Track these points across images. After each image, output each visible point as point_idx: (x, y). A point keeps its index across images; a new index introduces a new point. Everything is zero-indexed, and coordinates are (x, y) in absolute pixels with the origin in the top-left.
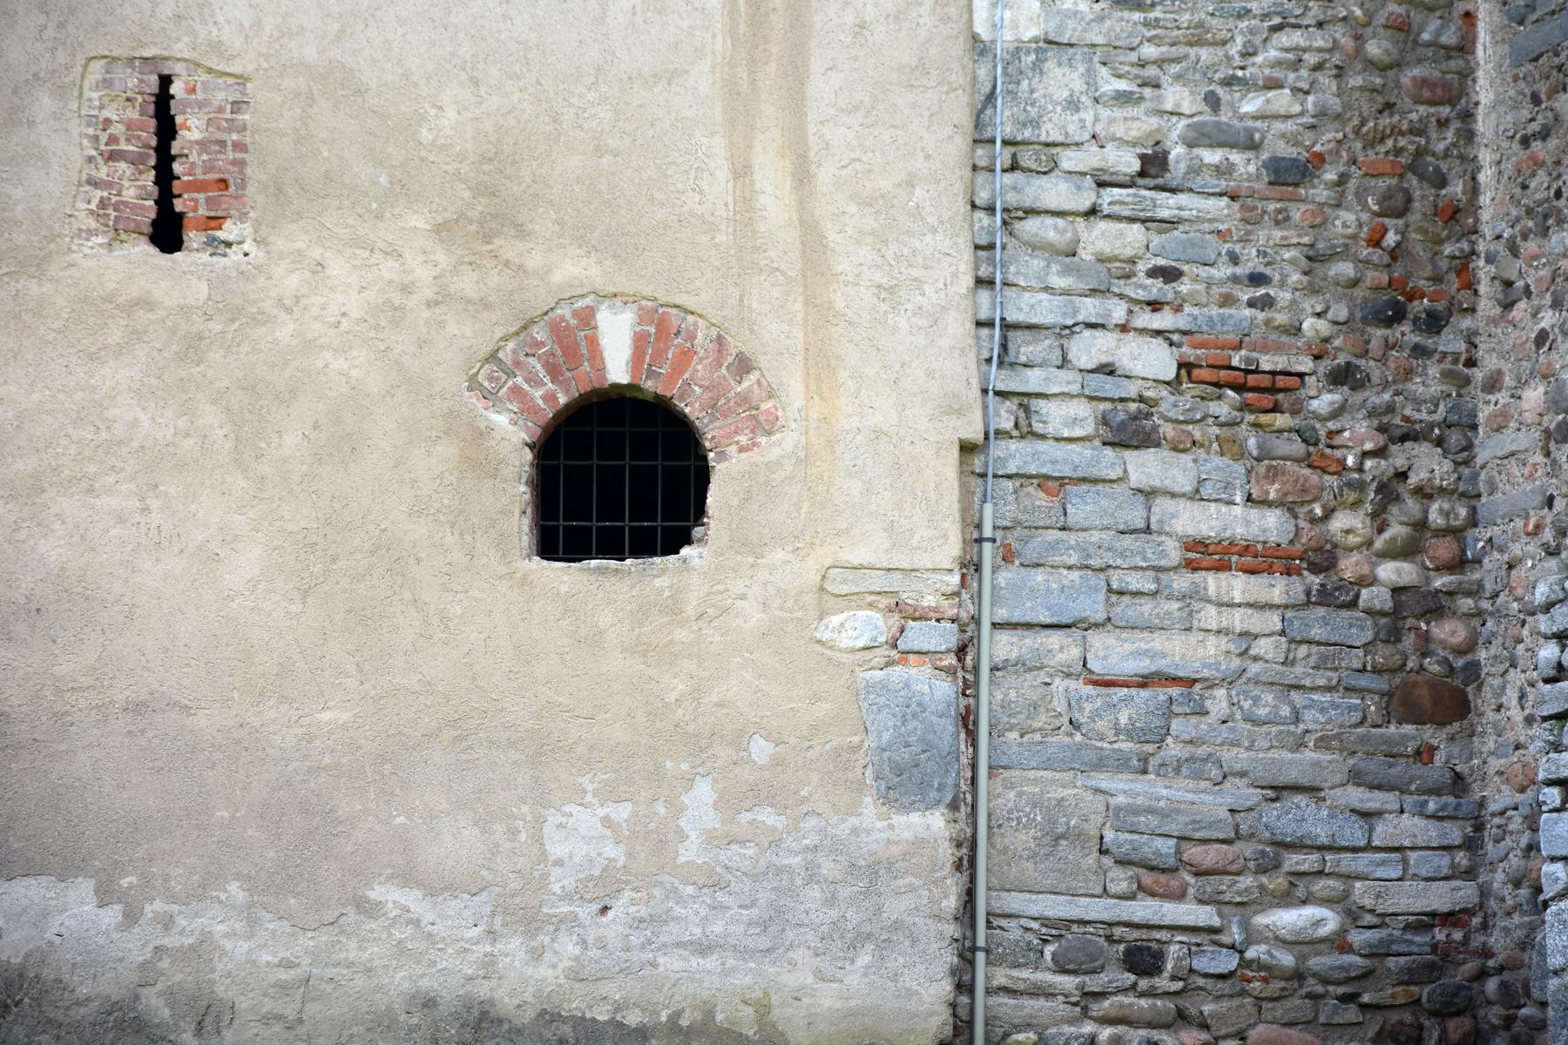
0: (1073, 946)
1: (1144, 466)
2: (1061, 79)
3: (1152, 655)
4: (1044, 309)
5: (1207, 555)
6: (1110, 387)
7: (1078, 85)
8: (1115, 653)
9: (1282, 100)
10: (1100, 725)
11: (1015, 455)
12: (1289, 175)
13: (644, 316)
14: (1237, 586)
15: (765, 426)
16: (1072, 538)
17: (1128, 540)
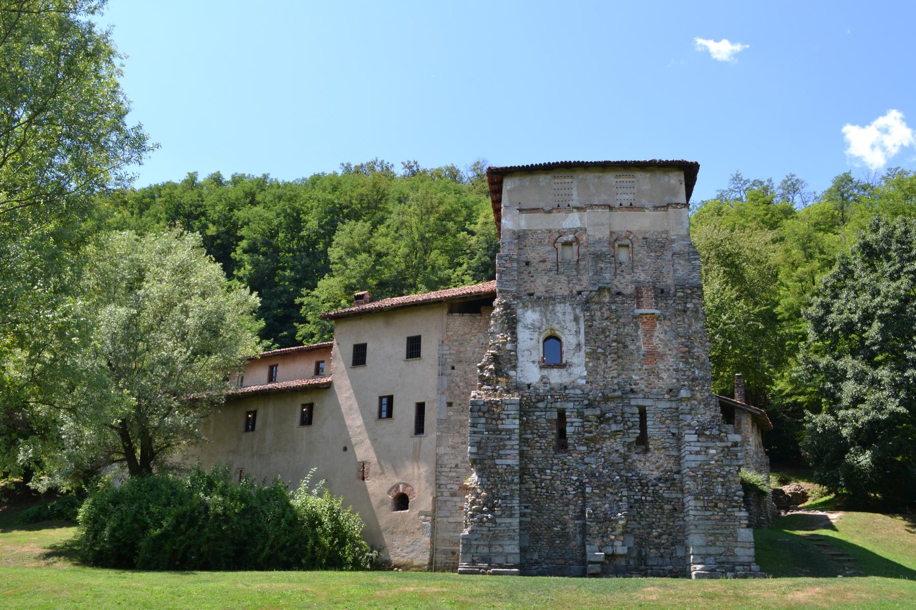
0: (445, 552)
1: (455, 499)
2: (446, 457)
8: (451, 520)
11: (440, 498)
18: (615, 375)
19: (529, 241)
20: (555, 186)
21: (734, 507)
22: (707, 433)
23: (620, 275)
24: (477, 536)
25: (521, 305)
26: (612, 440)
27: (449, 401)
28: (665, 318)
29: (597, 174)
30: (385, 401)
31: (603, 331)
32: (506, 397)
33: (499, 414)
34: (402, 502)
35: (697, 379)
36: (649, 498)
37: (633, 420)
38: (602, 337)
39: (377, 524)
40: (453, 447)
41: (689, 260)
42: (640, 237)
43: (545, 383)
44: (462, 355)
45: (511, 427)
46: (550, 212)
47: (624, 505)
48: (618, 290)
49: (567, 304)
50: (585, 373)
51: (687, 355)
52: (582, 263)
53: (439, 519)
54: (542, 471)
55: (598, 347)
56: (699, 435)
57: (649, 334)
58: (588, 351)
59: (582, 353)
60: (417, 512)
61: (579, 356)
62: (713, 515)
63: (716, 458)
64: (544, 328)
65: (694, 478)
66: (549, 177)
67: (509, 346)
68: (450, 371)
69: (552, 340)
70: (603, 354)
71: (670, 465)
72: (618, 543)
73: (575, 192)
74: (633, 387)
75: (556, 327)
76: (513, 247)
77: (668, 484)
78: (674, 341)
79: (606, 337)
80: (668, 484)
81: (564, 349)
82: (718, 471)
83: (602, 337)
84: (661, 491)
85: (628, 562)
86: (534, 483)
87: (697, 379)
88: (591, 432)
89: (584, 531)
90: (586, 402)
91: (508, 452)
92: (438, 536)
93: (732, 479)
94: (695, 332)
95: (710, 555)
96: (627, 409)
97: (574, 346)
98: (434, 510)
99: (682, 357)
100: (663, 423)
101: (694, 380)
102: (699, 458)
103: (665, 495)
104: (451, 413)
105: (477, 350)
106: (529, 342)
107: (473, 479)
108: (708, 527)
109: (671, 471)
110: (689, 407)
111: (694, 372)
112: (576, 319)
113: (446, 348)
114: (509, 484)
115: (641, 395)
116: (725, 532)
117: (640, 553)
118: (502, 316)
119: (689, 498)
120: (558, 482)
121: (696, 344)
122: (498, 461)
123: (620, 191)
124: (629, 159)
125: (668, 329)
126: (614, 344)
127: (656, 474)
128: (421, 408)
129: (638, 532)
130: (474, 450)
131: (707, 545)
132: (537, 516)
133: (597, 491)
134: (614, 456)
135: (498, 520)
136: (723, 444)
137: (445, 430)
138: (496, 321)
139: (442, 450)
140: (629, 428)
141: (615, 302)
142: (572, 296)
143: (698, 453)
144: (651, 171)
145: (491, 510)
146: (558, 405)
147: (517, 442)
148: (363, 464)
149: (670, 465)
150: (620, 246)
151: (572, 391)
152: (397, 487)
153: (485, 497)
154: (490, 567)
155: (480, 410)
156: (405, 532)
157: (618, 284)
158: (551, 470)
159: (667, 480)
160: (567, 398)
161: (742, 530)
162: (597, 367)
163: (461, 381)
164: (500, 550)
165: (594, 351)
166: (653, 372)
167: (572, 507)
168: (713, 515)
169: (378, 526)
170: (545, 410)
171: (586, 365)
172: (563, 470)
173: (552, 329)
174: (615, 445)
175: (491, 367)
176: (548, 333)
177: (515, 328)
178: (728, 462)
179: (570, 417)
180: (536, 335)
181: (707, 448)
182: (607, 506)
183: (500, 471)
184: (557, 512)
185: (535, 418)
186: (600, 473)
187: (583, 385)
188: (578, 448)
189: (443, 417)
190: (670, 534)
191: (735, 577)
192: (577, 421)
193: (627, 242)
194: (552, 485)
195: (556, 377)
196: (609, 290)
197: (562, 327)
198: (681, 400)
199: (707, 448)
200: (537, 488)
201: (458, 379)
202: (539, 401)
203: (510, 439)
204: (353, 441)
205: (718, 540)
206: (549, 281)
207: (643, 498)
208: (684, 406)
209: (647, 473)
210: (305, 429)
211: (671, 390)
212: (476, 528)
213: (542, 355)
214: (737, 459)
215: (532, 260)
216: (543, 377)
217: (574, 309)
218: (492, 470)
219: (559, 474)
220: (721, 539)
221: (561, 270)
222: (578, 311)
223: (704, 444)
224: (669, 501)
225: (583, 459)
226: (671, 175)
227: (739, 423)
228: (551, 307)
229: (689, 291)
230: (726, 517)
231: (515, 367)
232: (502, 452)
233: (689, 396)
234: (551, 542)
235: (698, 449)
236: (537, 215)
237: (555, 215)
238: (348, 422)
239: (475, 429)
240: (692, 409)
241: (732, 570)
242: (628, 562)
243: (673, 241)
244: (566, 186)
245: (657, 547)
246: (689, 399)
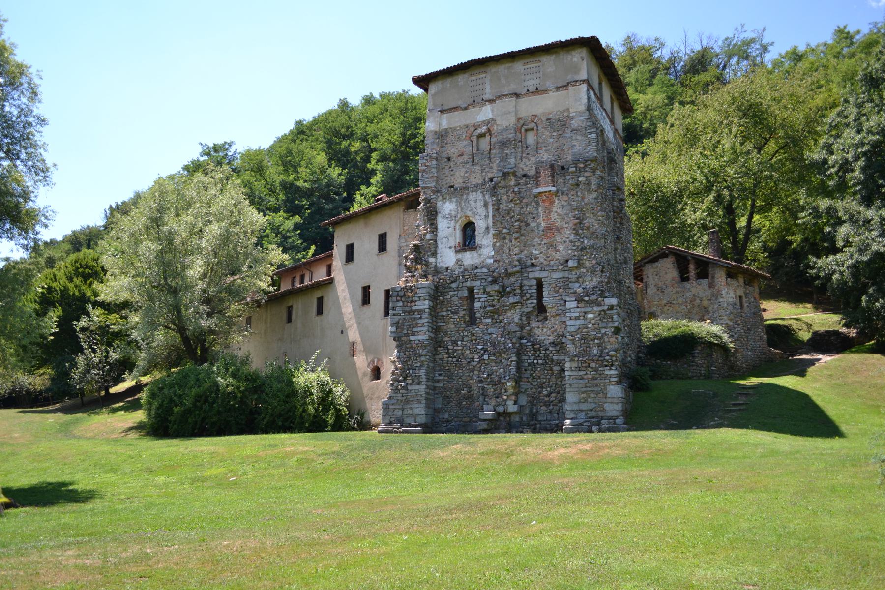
19: (450, 138)
20: (472, 84)
21: (606, 366)
23: (526, 158)
24: (393, 401)
25: (441, 198)
28: (563, 194)
29: (507, 65)
34: (376, 373)
35: (585, 248)
36: (540, 362)
37: (530, 291)
41: (585, 135)
42: (544, 119)
46: (466, 108)
48: (523, 173)
50: (493, 253)
51: (579, 226)
52: (493, 152)
54: (455, 343)
55: (504, 228)
57: (548, 211)
59: (491, 235)
62: (586, 374)
63: (593, 321)
64: (459, 216)
66: (466, 75)
72: (510, 403)
73: (488, 86)
74: (534, 261)
75: (469, 213)
76: (435, 146)
77: (558, 348)
80: (558, 348)
85: (521, 418)
86: (447, 353)
91: (419, 329)
94: (586, 204)
95: (582, 411)
100: (557, 292)
102: (578, 322)
103: (554, 358)
106: (448, 232)
111: (583, 242)
112: (486, 205)
113: (403, 241)
116: (596, 389)
117: (531, 409)
120: (468, 352)
121: (587, 215)
122: (412, 338)
123: (528, 77)
124: (532, 46)
127: (551, 339)
129: (530, 391)
130: (394, 329)
131: (580, 402)
134: (513, 327)
135: (409, 388)
136: (600, 308)
140: (528, 299)
141: (519, 184)
142: (484, 184)
143: (577, 318)
144: (556, 52)
146: (468, 284)
148: (353, 343)
150: (526, 130)
152: (373, 362)
154: (402, 426)
157: (523, 167)
158: (462, 341)
160: (475, 277)
161: (612, 387)
164: (410, 412)
167: (476, 372)
168: (586, 374)
170: (457, 289)
171: (494, 245)
172: (472, 341)
173: (466, 217)
174: (514, 316)
175: (412, 256)
177: (435, 219)
178: (604, 325)
179: (478, 293)
180: (453, 223)
181: (585, 313)
182: (502, 370)
191: (600, 431)
192: (483, 296)
193: (533, 125)
195: (469, 259)
196: (514, 174)
197: (474, 213)
199: (585, 313)
202: (452, 282)
203: (421, 318)
204: (347, 325)
206: (466, 172)
210: (319, 317)
214: (613, 321)
215: (452, 156)
216: (458, 260)
217: (484, 196)
220: (592, 396)
221: (476, 161)
222: (487, 197)
223: (583, 310)
226: (573, 53)
227: (713, 277)
228: (465, 196)
229: (582, 165)
231: (434, 254)
232: (414, 330)
234: (459, 404)
235: (577, 314)
236: (456, 113)
237: (472, 110)
238: (344, 310)
241: (599, 424)
242: (521, 418)
243: (572, 118)
244: (481, 81)
245: (547, 404)
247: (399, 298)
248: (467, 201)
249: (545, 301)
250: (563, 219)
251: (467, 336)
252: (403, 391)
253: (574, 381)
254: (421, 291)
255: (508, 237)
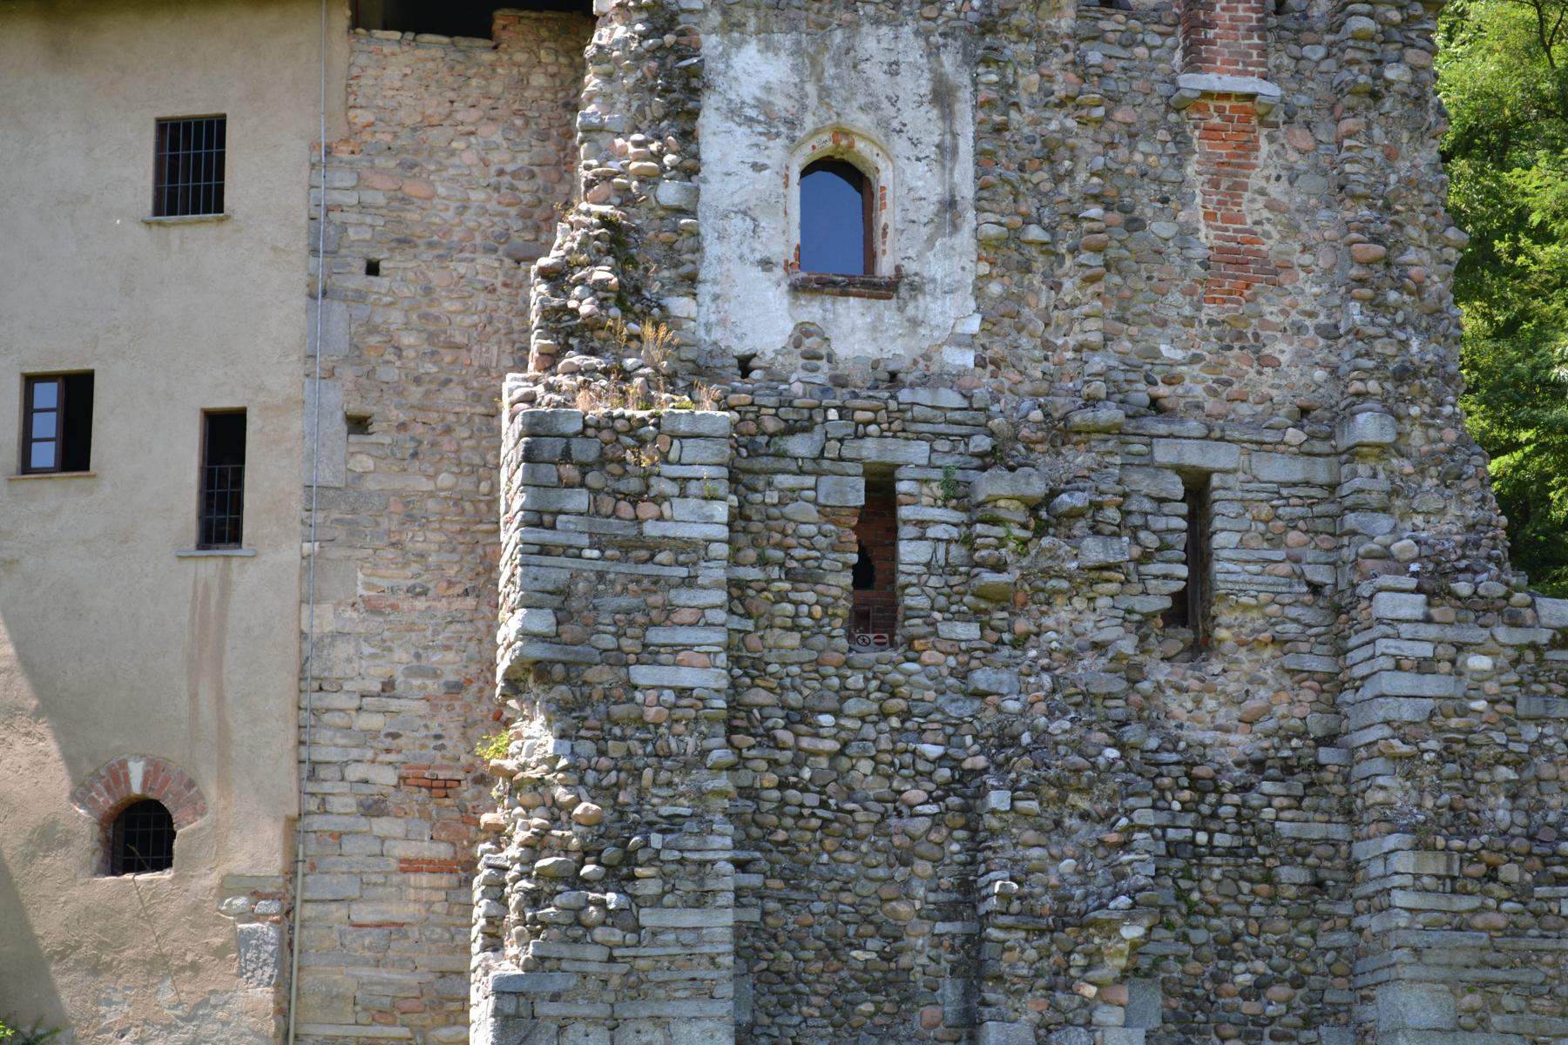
1: (381, 825)
2: (343, 649)
3: (383, 913)
4: (332, 754)
5: (410, 866)
6: (365, 789)
7: (352, 651)
8: (364, 913)
9: (450, 656)
10: (355, 946)
11: (317, 822)
12: (455, 689)
13: (150, 763)
14: (424, 879)
15: (202, 812)
16: (343, 860)
17: (371, 860)
18: (1096, 338)
22: (1463, 588)
24: (558, 982)
26: (1079, 603)
27: (357, 408)
28: (1290, 120)
30: (47, 395)
31: (1049, 157)
32: (670, 404)
33: (646, 476)
35: (1415, 373)
37: (1160, 523)
38: (1041, 176)
39: (26, 926)
40: (373, 609)
43: (812, 356)
44: (412, 216)
45: (697, 531)
47: (1140, 864)
49: (907, 31)
50: (974, 325)
51: (1377, 278)
53: (309, 911)
54: (800, 717)
55: (1027, 221)
56: (1431, 595)
57: (1229, 179)
58: (992, 231)
59: (964, 240)
60: (213, 880)
61: (949, 253)
63: (1492, 688)
64: (810, 122)
65: (1407, 765)
67: (669, 192)
68: (360, 280)
69: (841, 174)
70: (1046, 248)
71: (1298, 708)
74: (1162, 390)
75: (861, 121)
77: (1297, 785)
78: (1323, 215)
79: (1058, 179)
80: (1297, 785)
81: (887, 216)
82: (1500, 738)
83: (1041, 176)
84: (1268, 813)
86: (773, 764)
87: (1415, 373)
88: (999, 567)
89: (973, 965)
90: (982, 443)
91: (682, 636)
92: (308, 980)
93: (1548, 771)
94: (1408, 183)
96: (1141, 481)
97: (929, 210)
98: (291, 874)
99: (1361, 282)
100: (1275, 541)
101: (1404, 374)
103: (1286, 829)
104: (364, 463)
105: (477, 196)
106: (745, 180)
107: (532, 740)
108: (1461, 958)
109: (1303, 735)
110: (1382, 483)
111: (1404, 344)
112: (942, 96)
114: (687, 768)
115: (1194, 426)
116: (1524, 975)
118: (638, 58)
119: (1392, 841)
120: (865, 766)
121: (1412, 231)
122: (642, 674)
125: (1302, 164)
126: (1095, 211)
127: (1242, 743)
128: (225, 435)
129: (1176, 970)
130: (544, 622)
132: (785, 902)
133: (1033, 805)
135: (648, 918)
137: (340, 533)
138: (609, 77)
139: (324, 619)
140: (1146, 557)
141: (1098, 37)
143: (1423, 666)
145: (620, 874)
146: (871, 449)
147: (720, 597)
149: (1298, 708)
151: (923, 396)
153: (590, 822)
155: (566, 456)
156: (158, 966)
158: (837, 713)
159: (1288, 770)
160: (901, 424)
162: (1020, 299)
163: (407, 326)
165: (1014, 237)
166: (1240, 336)
167: (923, 868)
168: (1483, 909)
169: (31, 940)
171: (978, 291)
172: (884, 715)
173: (839, 132)
175: (601, 273)
176: (823, 145)
177: (694, 115)
178: (1536, 706)
179: (914, 500)
180: (777, 148)
181: (1460, 647)
182: (1068, 865)
183: (651, 713)
184: (866, 888)
185: (772, 497)
186: (1040, 736)
187: (962, 373)
188: (945, 629)
189: (326, 476)
190: (1297, 982)
192: (945, 520)
194: (841, 776)
195: (858, 332)
197: (883, 124)
198: (1354, 453)
199: (1460, 647)
200: (782, 786)
201: (396, 317)
202: (790, 430)
203: (689, 582)
205: (1497, 1008)
207: (1202, 837)
208: (1363, 479)
209: (1208, 737)
211: (1305, 412)
212: (555, 950)
213: (796, 239)
216: (804, 331)
217: (933, 52)
218: (618, 711)
219: (869, 732)
220: (1510, 1002)
222: (949, 62)
223: (1451, 633)
224: (1298, 851)
225: (963, 674)
228: (838, 37)
230: (1527, 920)
231: (690, 282)
232: (656, 636)
233: (1389, 438)
235: (1426, 650)
239: (546, 536)
240: (1394, 492)
246: (1382, 450)
247: (570, 472)
248: (849, 58)
249: (1227, 569)
250: (1293, 228)
251: (860, 693)
252: (616, 935)
253: (1434, 937)
254: (691, 450)
255: (1040, 264)
